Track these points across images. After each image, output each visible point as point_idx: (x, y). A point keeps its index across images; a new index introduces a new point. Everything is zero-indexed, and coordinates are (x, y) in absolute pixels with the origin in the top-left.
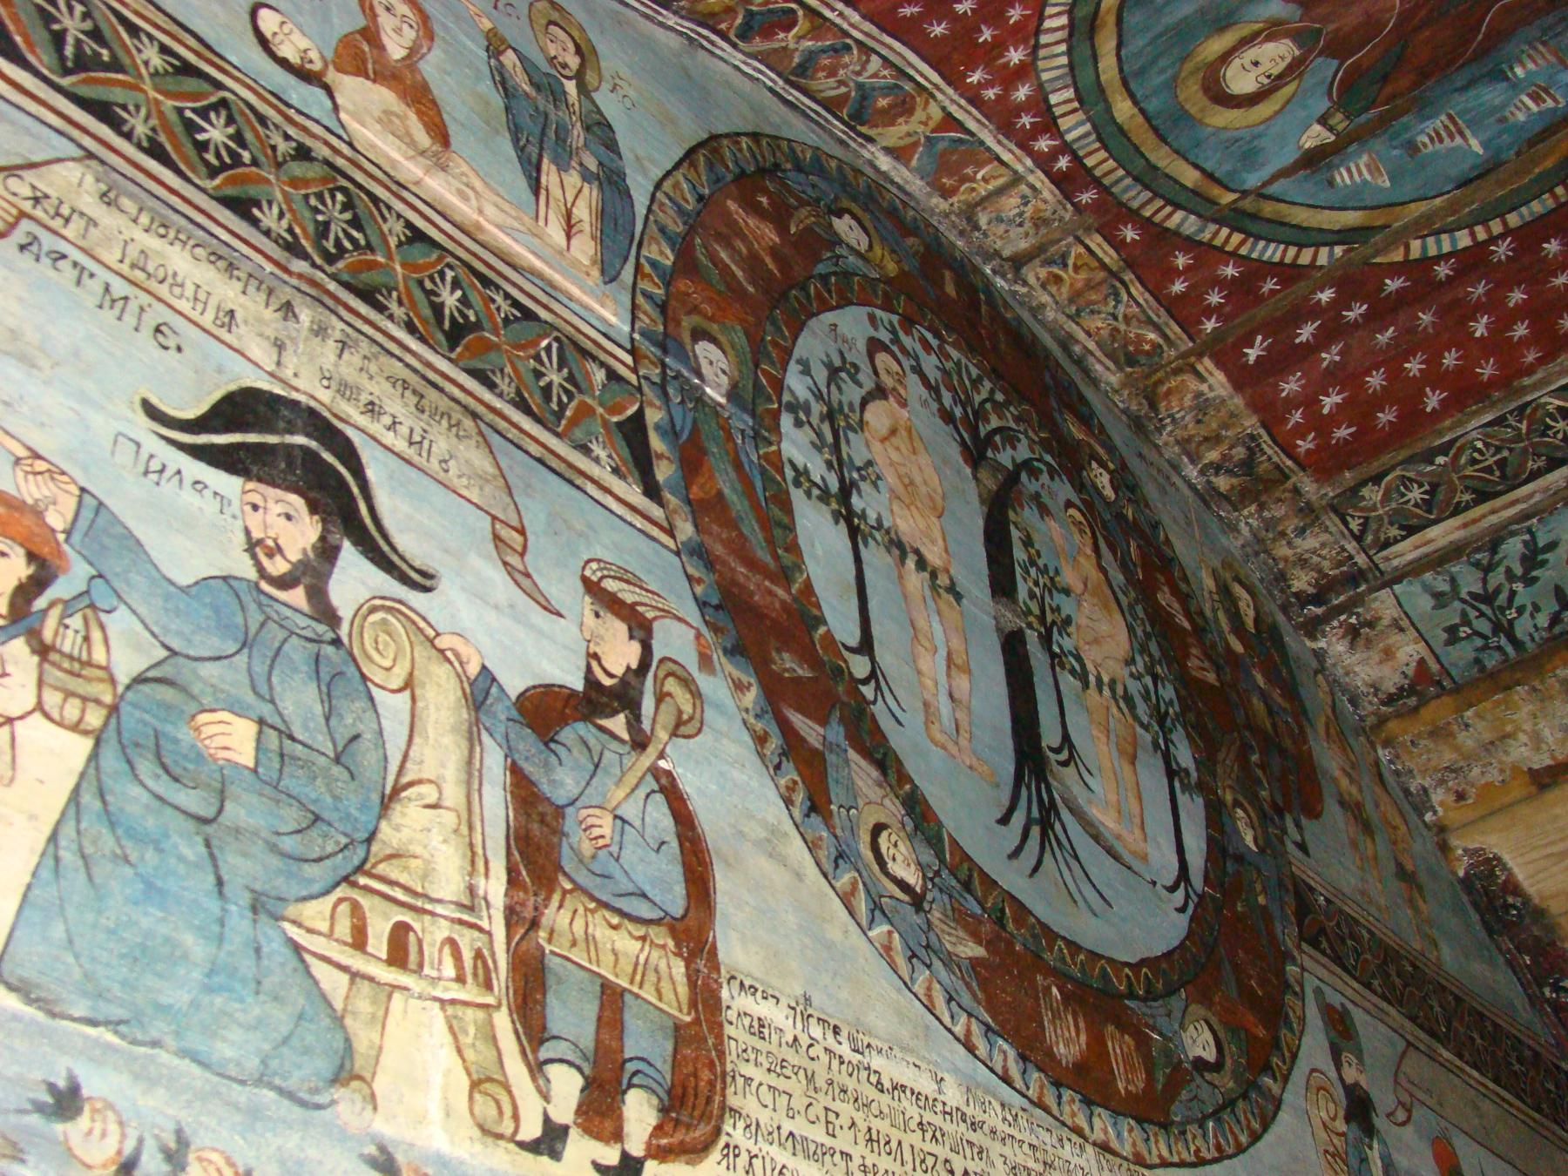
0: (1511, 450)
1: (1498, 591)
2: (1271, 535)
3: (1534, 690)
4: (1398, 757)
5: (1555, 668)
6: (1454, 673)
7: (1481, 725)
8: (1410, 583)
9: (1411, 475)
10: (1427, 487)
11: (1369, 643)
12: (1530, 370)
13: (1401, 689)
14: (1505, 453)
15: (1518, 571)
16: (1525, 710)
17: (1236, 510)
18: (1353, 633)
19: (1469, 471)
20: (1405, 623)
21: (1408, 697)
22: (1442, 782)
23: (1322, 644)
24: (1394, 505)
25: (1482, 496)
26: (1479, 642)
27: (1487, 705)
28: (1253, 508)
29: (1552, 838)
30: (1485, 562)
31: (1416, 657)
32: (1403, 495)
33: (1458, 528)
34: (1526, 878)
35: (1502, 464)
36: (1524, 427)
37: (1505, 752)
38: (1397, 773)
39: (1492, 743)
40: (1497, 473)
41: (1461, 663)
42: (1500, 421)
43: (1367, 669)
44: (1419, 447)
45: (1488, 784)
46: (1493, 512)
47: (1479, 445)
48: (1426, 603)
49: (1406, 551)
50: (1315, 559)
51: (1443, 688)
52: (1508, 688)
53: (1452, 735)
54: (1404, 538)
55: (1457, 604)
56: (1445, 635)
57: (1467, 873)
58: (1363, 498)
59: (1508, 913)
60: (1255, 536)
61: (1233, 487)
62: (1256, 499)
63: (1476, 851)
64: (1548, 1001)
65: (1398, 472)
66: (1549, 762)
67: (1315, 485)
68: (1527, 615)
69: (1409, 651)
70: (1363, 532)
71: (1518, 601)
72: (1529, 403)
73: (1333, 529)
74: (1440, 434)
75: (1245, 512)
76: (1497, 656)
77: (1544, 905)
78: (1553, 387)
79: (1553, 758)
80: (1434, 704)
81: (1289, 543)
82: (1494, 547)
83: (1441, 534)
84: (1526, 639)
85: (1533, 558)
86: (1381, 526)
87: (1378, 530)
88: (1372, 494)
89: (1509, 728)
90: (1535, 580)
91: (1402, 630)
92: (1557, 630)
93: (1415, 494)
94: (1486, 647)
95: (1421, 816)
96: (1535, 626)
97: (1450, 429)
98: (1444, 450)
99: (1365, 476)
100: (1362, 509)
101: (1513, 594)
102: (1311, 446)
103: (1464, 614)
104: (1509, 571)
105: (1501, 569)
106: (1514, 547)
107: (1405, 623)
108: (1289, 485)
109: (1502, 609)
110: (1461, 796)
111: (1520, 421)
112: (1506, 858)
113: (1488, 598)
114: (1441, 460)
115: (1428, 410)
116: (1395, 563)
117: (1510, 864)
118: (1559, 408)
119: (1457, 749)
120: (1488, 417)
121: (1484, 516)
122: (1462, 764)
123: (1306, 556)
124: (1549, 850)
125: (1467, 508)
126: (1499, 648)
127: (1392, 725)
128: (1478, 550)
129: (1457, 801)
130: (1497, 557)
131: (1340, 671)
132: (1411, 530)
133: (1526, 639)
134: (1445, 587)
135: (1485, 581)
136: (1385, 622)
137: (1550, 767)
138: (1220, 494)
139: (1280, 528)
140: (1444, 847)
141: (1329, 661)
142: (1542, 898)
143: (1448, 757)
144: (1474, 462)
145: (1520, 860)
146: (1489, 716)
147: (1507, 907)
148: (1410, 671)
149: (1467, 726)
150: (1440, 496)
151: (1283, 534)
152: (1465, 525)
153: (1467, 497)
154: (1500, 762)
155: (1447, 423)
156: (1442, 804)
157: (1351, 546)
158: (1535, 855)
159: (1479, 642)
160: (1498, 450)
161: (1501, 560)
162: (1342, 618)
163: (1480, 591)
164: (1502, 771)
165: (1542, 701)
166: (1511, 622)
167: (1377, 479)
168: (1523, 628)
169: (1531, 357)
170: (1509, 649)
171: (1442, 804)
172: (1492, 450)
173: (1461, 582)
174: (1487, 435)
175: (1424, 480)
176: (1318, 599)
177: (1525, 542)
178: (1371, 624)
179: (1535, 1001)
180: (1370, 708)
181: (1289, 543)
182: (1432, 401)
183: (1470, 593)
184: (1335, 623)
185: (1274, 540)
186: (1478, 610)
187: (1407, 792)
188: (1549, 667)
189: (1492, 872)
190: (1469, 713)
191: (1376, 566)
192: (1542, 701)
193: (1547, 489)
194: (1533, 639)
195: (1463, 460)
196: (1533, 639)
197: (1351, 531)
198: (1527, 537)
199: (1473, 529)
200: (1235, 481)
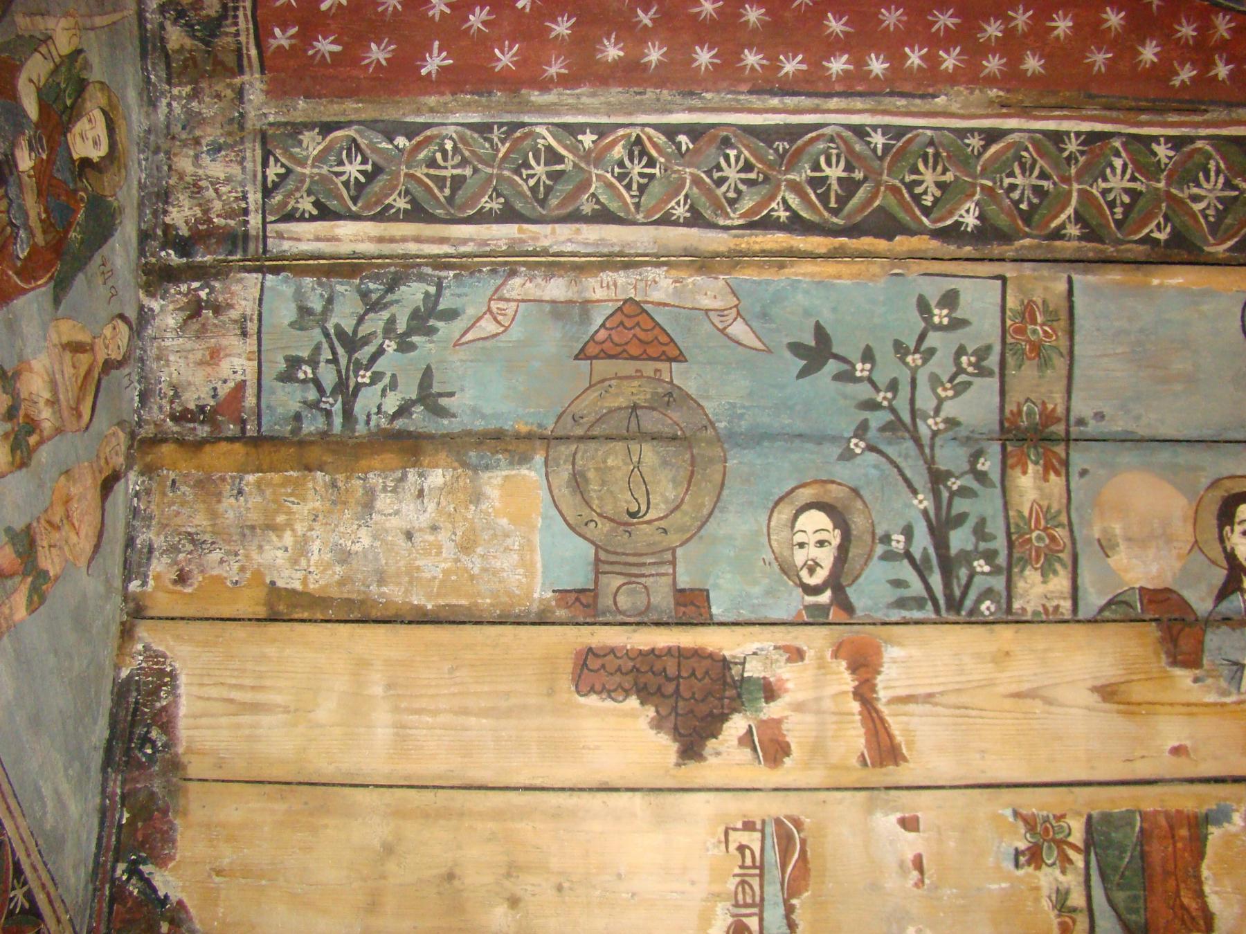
0: (476, 170)
1: (366, 340)
2: (184, 136)
3: (334, 485)
4: (148, 492)
5: (370, 469)
6: (264, 420)
7: (254, 500)
8: (286, 280)
9: (362, 142)
10: (369, 167)
11: (201, 334)
12: (544, 86)
13: (201, 409)
14: (468, 171)
15: (401, 327)
16: (310, 505)
17: (169, 83)
18: (195, 309)
19: (420, 172)
20: (252, 327)
21: (202, 422)
22: (174, 549)
23: (155, 305)
24: (325, 170)
25: (417, 213)
26: (312, 395)
27: (275, 477)
28: (188, 89)
29: (247, 682)
30: (374, 296)
31: (239, 377)
32: (341, 163)
33: (370, 239)
34: (185, 716)
35: (458, 182)
36: (503, 150)
37: (260, 547)
38: (135, 512)
39: (253, 528)
40: (447, 191)
41: (280, 410)
42: (483, 129)
43: (182, 362)
44: (391, 113)
45: (219, 580)
46: (418, 240)
47: (449, 145)
48: (288, 313)
49: (305, 237)
50: (211, 193)
51: (243, 430)
52: (308, 469)
53: (219, 496)
54: (313, 219)
55: (317, 334)
56: (283, 366)
57: (130, 677)
58: (300, 142)
59: (141, 748)
60: (168, 127)
61: (182, 49)
62: (195, 82)
63: (157, 655)
64: (113, 881)
65: (351, 132)
66: (298, 586)
67: (262, 97)
68: (380, 386)
69: (237, 364)
70: (276, 186)
71: (377, 367)
72: (523, 125)
73: (249, 165)
74: (418, 112)
75: (175, 91)
76: (320, 423)
77: (185, 759)
78: (556, 120)
79: (305, 582)
80: (224, 446)
81: (197, 157)
82: (393, 284)
83: (352, 236)
84: (362, 418)
85: (422, 321)
86: (298, 189)
87: (289, 195)
88: (312, 143)
89: (281, 519)
90: (412, 347)
91: (244, 334)
92: (399, 424)
93: (353, 169)
94: (315, 405)
95: (127, 579)
96: (379, 407)
97: (432, 110)
98: (411, 131)
99: (316, 118)
100: (292, 157)
101: (381, 351)
102: (285, 43)
103: (317, 349)
104: (392, 321)
105: (385, 315)
106: (413, 293)
107: (252, 327)
108: (237, 80)
109: (358, 366)
110: (182, 578)
111: (503, 141)
112: (183, 679)
113: (351, 342)
114: (401, 141)
115: (424, 72)
116: (286, 245)
117: (182, 690)
118: (549, 148)
119: (213, 515)
120: (475, 118)
121: (404, 240)
122: (207, 537)
123: (203, 183)
124: (235, 695)
125: (395, 218)
126: (328, 414)
127: (166, 449)
128: (376, 278)
129: (175, 582)
130: (390, 297)
131: (152, 352)
132: (325, 213)
133: (362, 418)
134: (317, 306)
135: (361, 320)
136: (234, 314)
137: (294, 591)
138: (164, 48)
139: (198, 133)
140: (127, 633)
141: (150, 331)
142: (189, 750)
143: (199, 521)
144: (432, 163)
145: (195, 690)
146: (268, 492)
147: (146, 740)
148: (224, 391)
149: (240, 492)
150: (377, 186)
151: (197, 142)
152: (381, 240)
153: (402, 204)
154: (247, 556)
155: (432, 100)
156: (157, 578)
157: (254, 197)
158: (214, 692)
159: (312, 395)
160: (464, 162)
161: (391, 303)
162: (195, 285)
163: (349, 330)
164: (242, 569)
165: (334, 503)
166: (358, 387)
167: (327, 128)
168: (366, 402)
169: (553, 70)
170: (338, 421)
171: (157, 578)
172: (458, 159)
173: (337, 307)
174: (463, 139)
175: (373, 157)
176: (184, 246)
177: (427, 294)
178: (217, 309)
179: (99, 872)
180: (157, 415)
181: (197, 157)
182: (434, 63)
183: (337, 326)
184: (184, 288)
185: (185, 144)
186: (334, 353)
187: (130, 542)
188: (364, 463)
189: (158, 689)
190: (251, 478)
191: (265, 237)
192: (334, 503)
193: (485, 243)
194: (368, 422)
195: (421, 156)
196: (368, 422)
197: (265, 177)
198: (432, 290)
199: (387, 249)
200: (188, 42)
